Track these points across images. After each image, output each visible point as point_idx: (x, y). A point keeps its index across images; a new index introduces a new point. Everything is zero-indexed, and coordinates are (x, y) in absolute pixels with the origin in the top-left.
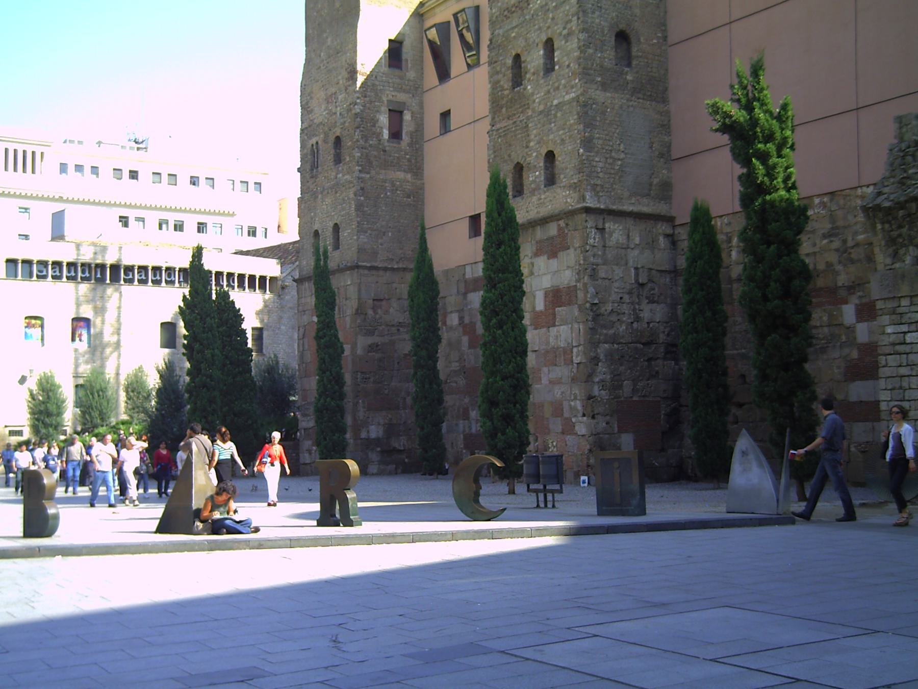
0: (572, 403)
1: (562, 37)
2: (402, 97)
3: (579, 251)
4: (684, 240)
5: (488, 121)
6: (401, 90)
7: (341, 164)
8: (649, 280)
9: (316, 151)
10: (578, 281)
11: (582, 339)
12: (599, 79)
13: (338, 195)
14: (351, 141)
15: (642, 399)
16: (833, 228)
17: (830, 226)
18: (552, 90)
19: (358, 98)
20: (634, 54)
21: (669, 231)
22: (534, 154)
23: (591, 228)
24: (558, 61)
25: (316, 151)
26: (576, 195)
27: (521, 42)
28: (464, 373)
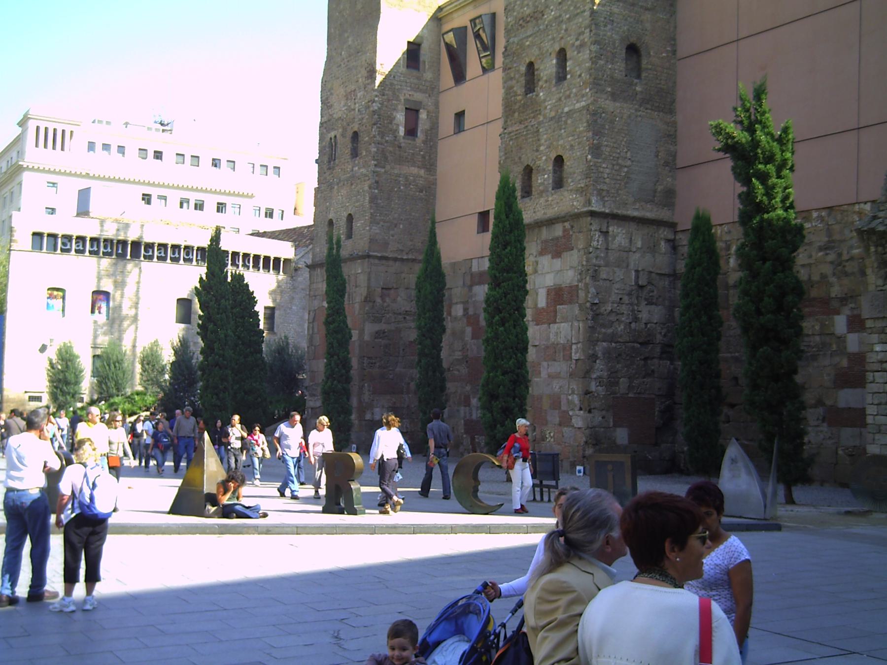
0: (570, 397)
1: (574, 48)
2: (418, 96)
3: (582, 252)
4: (685, 245)
5: (500, 123)
6: (417, 89)
7: (358, 158)
8: (648, 283)
9: (334, 144)
10: (580, 281)
11: (581, 337)
12: (609, 89)
13: (353, 187)
14: (368, 136)
15: (637, 395)
16: (829, 242)
17: (827, 239)
18: (563, 99)
19: (376, 96)
20: (643, 66)
21: (671, 236)
22: (544, 158)
23: (596, 230)
24: (570, 70)
25: (334, 144)
26: (582, 199)
27: (535, 51)
28: (467, 362)
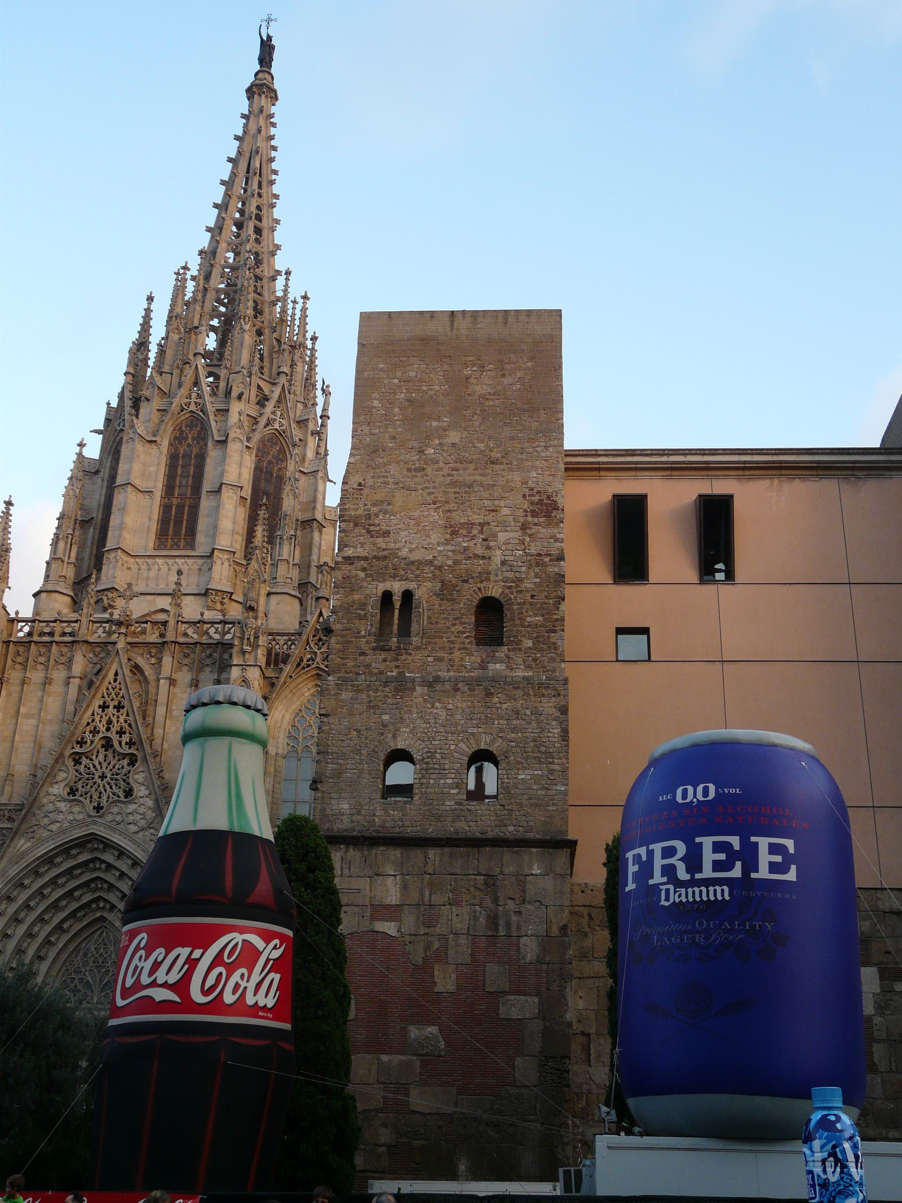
13: (496, 700)
